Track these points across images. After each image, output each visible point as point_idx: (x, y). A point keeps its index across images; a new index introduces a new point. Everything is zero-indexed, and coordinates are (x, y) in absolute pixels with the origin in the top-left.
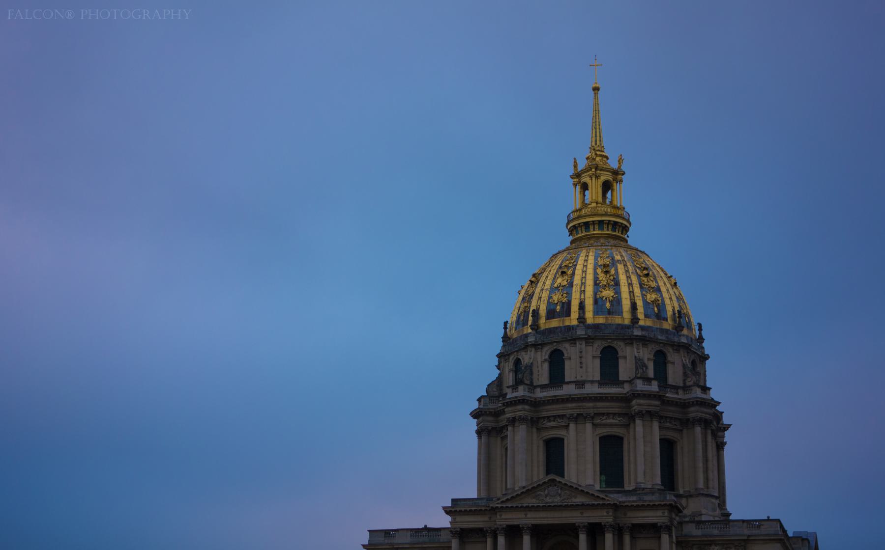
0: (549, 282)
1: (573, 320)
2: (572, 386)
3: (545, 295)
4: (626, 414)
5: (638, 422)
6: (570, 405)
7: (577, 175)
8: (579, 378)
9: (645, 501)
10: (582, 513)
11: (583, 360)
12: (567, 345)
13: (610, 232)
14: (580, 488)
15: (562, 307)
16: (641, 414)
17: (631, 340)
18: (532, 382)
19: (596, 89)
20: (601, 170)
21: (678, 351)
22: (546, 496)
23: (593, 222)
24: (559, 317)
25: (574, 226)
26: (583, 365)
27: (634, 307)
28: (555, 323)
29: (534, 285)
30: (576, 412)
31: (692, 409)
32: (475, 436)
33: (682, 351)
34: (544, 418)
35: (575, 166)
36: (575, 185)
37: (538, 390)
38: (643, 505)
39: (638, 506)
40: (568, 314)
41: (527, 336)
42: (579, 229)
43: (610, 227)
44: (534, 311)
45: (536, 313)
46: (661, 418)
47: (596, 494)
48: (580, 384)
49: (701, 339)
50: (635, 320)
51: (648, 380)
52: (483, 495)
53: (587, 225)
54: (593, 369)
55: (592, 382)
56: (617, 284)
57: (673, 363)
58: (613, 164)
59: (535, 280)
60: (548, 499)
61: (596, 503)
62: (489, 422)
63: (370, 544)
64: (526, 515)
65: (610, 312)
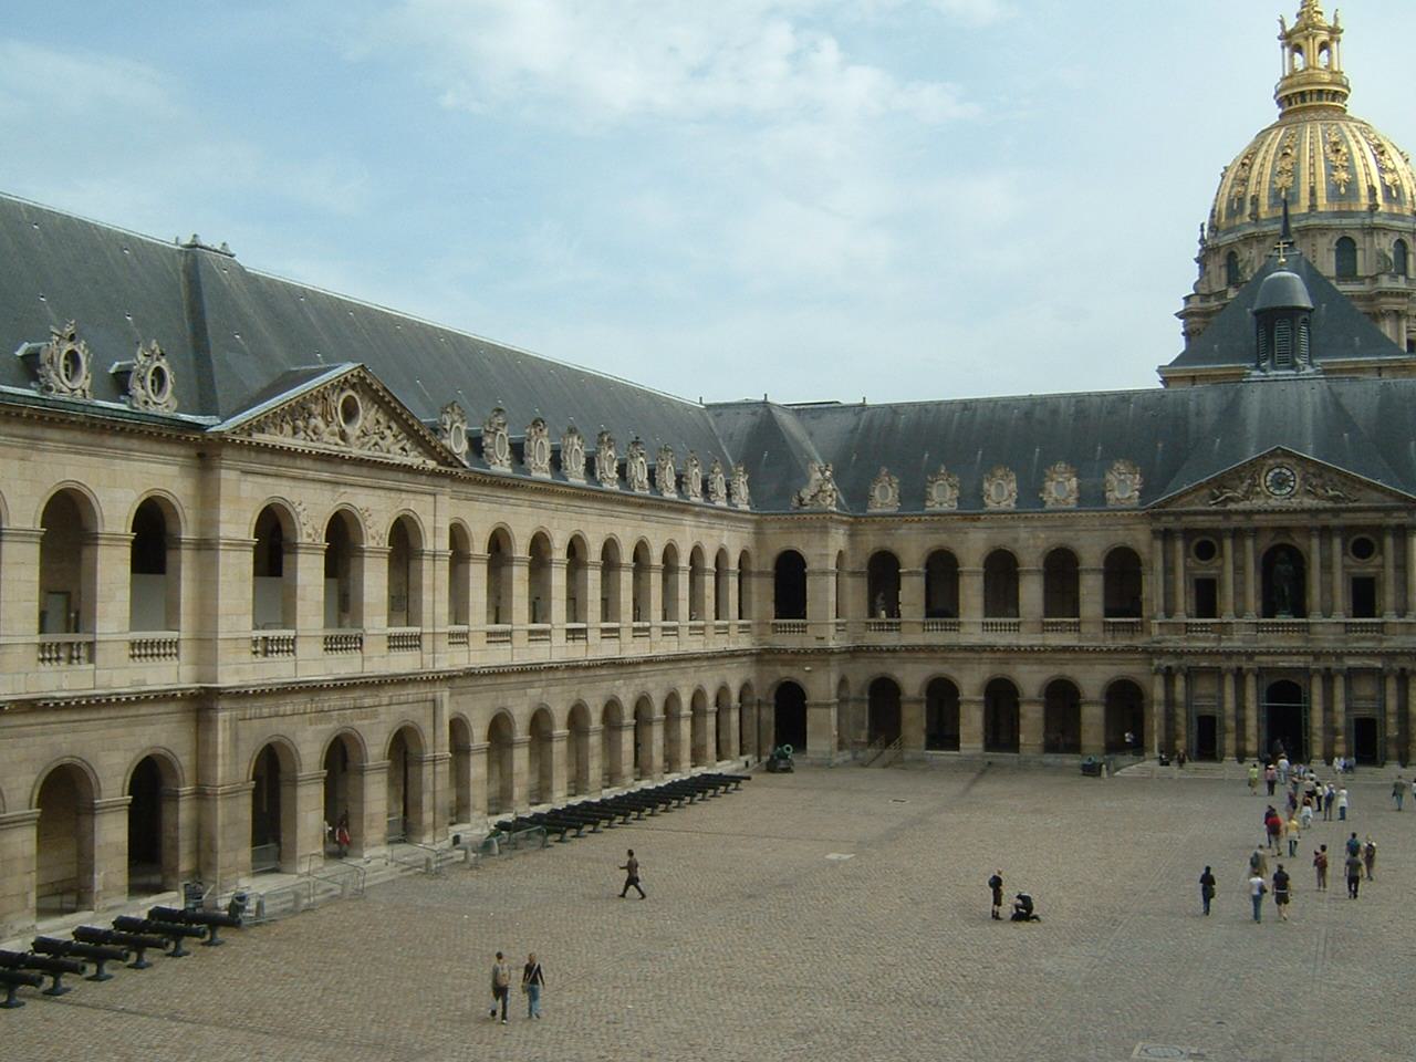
0: (1269, 165)
3: (1266, 178)
4: (1369, 314)
7: (1286, 37)
17: (1372, 230)
27: (1372, 190)
29: (1246, 168)
32: (1183, 338)
36: (1283, 47)
42: (1293, 100)
44: (1253, 197)
45: (1255, 200)
50: (1373, 207)
51: (1394, 277)
53: (1302, 94)
58: (1328, 21)
59: (1247, 161)
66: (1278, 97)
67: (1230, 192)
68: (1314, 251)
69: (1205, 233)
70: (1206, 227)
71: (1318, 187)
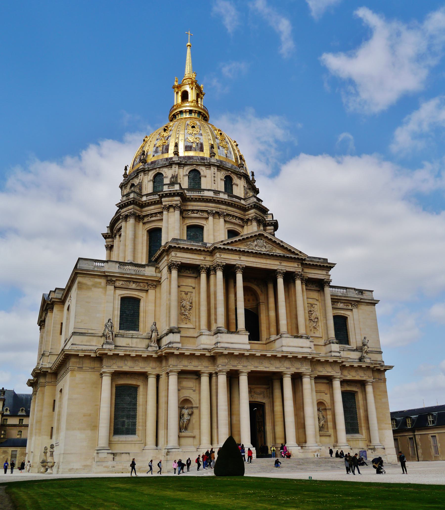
1: (206, 154)
6: (211, 205)
11: (216, 179)
12: (203, 168)
14: (281, 244)
22: (256, 246)
23: (195, 112)
24: (195, 150)
25: (181, 112)
30: (215, 210)
34: (189, 210)
38: (316, 265)
40: (202, 150)
42: (184, 114)
43: (203, 118)
44: (176, 143)
45: (176, 145)
53: (191, 112)
54: (221, 186)
56: (227, 142)
60: (257, 248)
61: (293, 256)
65: (227, 156)
68: (214, 177)
70: (128, 169)
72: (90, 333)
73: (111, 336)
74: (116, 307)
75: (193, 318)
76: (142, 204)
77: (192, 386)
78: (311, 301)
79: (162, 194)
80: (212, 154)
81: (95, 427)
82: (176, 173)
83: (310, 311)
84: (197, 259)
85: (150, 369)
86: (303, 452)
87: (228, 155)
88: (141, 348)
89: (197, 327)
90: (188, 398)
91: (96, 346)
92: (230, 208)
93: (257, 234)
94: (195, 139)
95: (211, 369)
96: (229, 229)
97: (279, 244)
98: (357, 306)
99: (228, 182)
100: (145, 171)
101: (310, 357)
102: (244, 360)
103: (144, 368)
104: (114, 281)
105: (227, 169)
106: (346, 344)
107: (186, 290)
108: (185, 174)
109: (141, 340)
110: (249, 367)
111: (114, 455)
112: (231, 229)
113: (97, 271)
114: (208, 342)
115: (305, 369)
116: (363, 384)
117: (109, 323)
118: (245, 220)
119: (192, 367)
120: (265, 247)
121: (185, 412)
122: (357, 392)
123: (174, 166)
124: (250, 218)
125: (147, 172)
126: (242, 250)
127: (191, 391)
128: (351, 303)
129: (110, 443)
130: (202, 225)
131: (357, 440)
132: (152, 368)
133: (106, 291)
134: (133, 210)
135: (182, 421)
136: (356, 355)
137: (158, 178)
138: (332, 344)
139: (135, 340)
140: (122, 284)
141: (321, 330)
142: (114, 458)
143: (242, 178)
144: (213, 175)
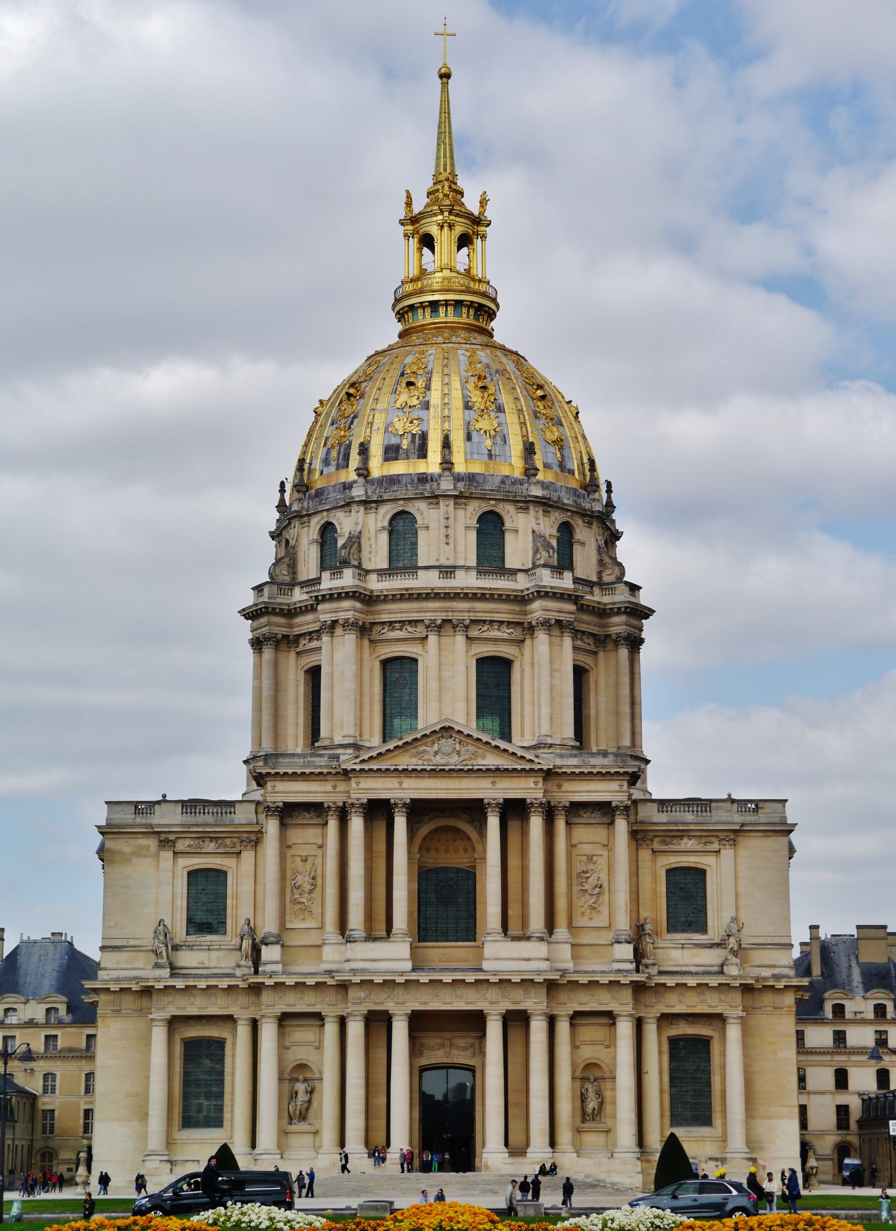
1: (432, 464)
2: (435, 573)
5: (542, 637)
6: (431, 605)
8: (444, 562)
9: (594, 766)
10: (494, 783)
11: (451, 532)
12: (422, 505)
13: (471, 321)
15: (413, 441)
16: (546, 625)
17: (524, 504)
18: (360, 564)
19: (445, 76)
20: (457, 215)
21: (590, 524)
22: (436, 753)
23: (447, 303)
25: (412, 307)
26: (446, 538)
27: (529, 450)
28: (399, 468)
30: (439, 617)
31: (616, 619)
33: (595, 523)
34: (384, 623)
35: (409, 204)
37: (373, 577)
39: (582, 773)
40: (423, 453)
41: (347, 486)
42: (420, 311)
43: (472, 312)
44: (362, 444)
45: (364, 450)
46: (576, 634)
47: (519, 754)
48: (448, 571)
49: (610, 506)
52: (267, 747)
53: (434, 306)
54: (466, 548)
55: (468, 568)
56: (500, 409)
57: (583, 544)
58: (471, 204)
59: (352, 391)
60: (438, 757)
61: (519, 767)
62: (277, 626)
63: (109, 825)
64: (401, 783)
65: (490, 456)
66: (397, 309)
67: (327, 439)
68: (447, 527)
69: (287, 496)
70: (288, 488)
71: (452, 438)
72: (131, 946)
73: (164, 953)
74: (179, 891)
75: (317, 910)
76: (289, 610)
77: (313, 1040)
78: (587, 849)
79: (316, 597)
80: (444, 465)
81: (144, 1116)
82: (359, 528)
83: (584, 872)
84: (316, 792)
85: (238, 1009)
86: (512, 1164)
87: (496, 451)
88: (226, 968)
89: (322, 927)
90: (304, 1062)
91: (143, 969)
92: (479, 605)
93: (437, 728)
94: (408, 424)
95: (340, 1011)
96: (481, 656)
97: (487, 743)
98: (734, 843)
99: (491, 529)
100: (302, 517)
101: (539, 979)
102: (400, 991)
103: (227, 1008)
104: (172, 841)
105: (483, 499)
106: (697, 931)
107: (304, 853)
108: (380, 525)
109: (227, 952)
110: (410, 1004)
111: (172, 1164)
112: (486, 655)
113: (140, 825)
114: (337, 957)
115: (534, 1003)
116: (719, 1019)
117: (161, 928)
118: (526, 625)
119: (304, 1006)
120: (458, 753)
121: (301, 1087)
122: (712, 1037)
123: (355, 508)
124: (534, 623)
125: (305, 519)
126: (400, 768)
127: (311, 1049)
128: (717, 836)
129: (170, 1143)
130: (414, 656)
131: (702, 1139)
132: (242, 1008)
133: (158, 862)
134: (267, 628)
135: (293, 1104)
136: (711, 958)
137: (328, 536)
138: (616, 946)
139: (214, 954)
140: (189, 846)
141: (605, 912)
142: (171, 1170)
143: (531, 507)
144: (443, 522)
